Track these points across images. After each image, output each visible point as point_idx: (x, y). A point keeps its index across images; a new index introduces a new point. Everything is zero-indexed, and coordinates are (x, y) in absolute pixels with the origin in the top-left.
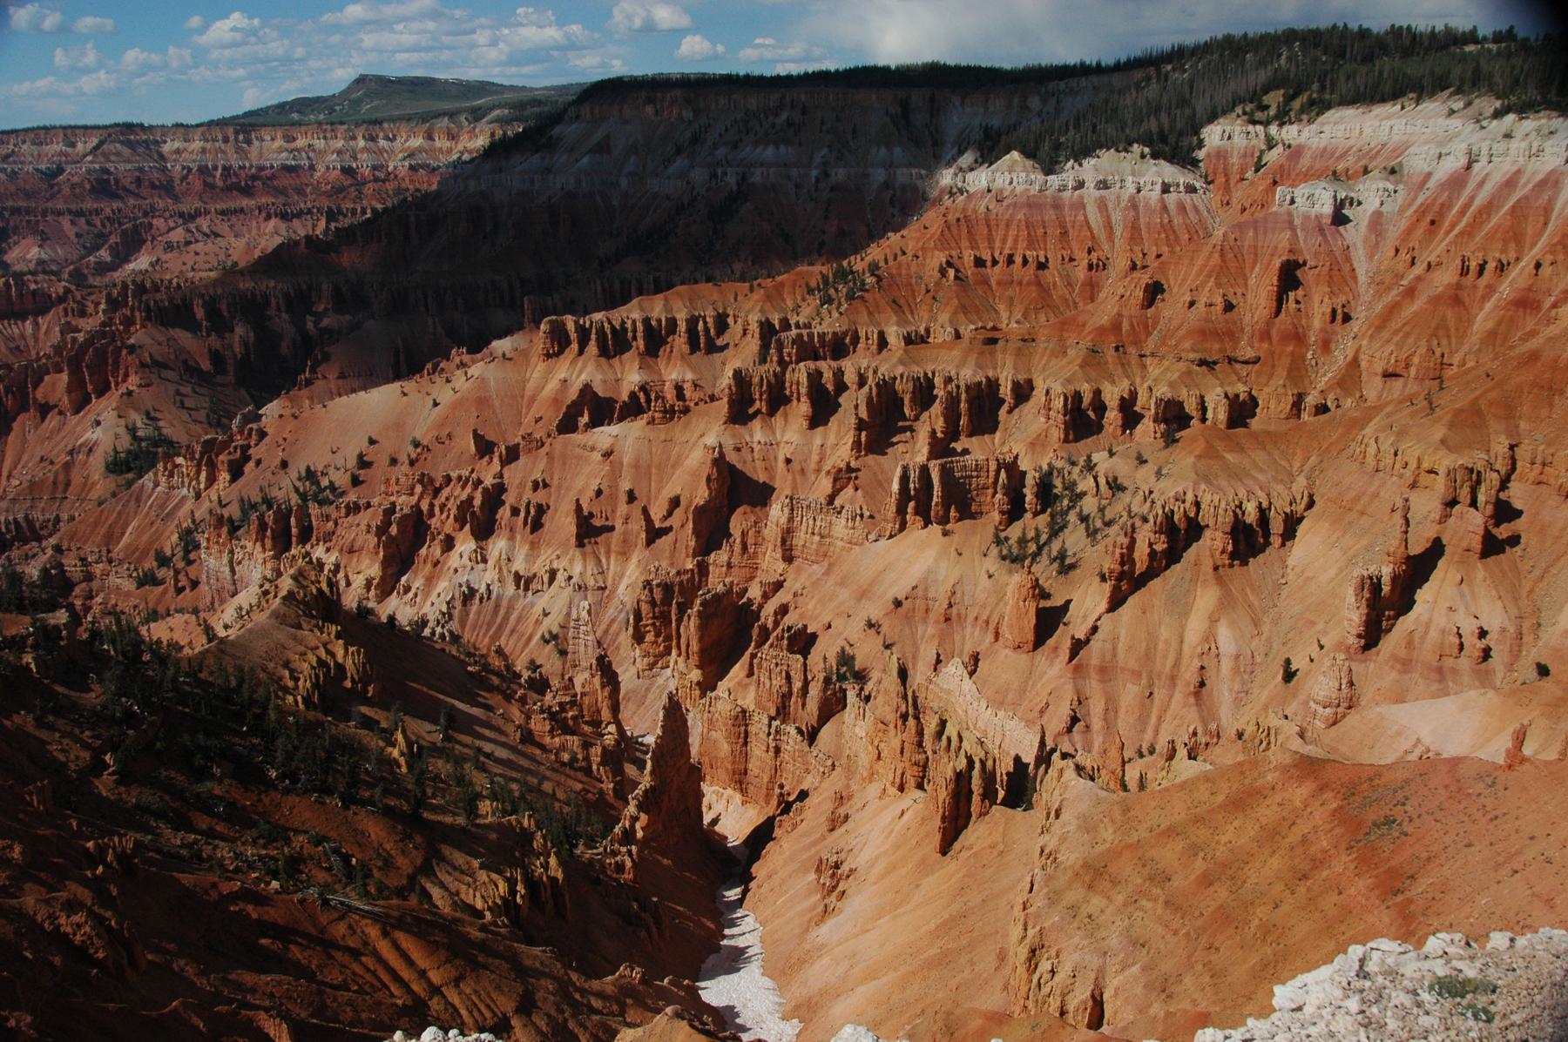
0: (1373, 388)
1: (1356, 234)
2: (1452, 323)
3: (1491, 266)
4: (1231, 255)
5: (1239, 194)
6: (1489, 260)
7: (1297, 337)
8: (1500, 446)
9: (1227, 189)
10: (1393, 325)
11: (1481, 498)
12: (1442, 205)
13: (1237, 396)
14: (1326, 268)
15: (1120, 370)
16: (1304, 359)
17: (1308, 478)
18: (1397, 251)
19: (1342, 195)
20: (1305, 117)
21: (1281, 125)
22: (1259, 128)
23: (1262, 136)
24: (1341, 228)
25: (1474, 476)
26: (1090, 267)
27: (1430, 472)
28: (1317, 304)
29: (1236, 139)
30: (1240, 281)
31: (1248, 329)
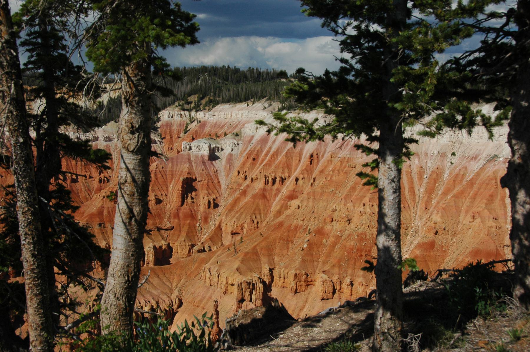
0: (227, 240)
1: (220, 165)
2: (261, 208)
3: (278, 180)
4: (160, 176)
5: (177, 144)
6: (277, 177)
7: (192, 216)
8: (265, 270)
9: (171, 142)
10: (237, 209)
11: (254, 297)
12: (258, 151)
13: (161, 247)
14: (206, 182)
15: (101, 236)
16: (195, 227)
17: (179, 291)
18: (239, 173)
19: (213, 146)
20: (207, 108)
21: (196, 111)
22: (187, 113)
23: (188, 116)
24: (214, 162)
25: (251, 286)
26: (100, 181)
27: (232, 285)
28: (202, 199)
29: (175, 117)
30: (164, 188)
31: (168, 213)
